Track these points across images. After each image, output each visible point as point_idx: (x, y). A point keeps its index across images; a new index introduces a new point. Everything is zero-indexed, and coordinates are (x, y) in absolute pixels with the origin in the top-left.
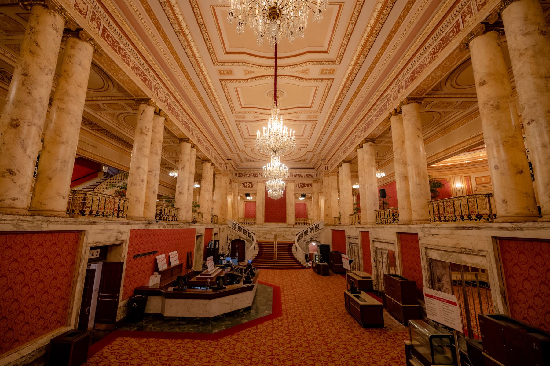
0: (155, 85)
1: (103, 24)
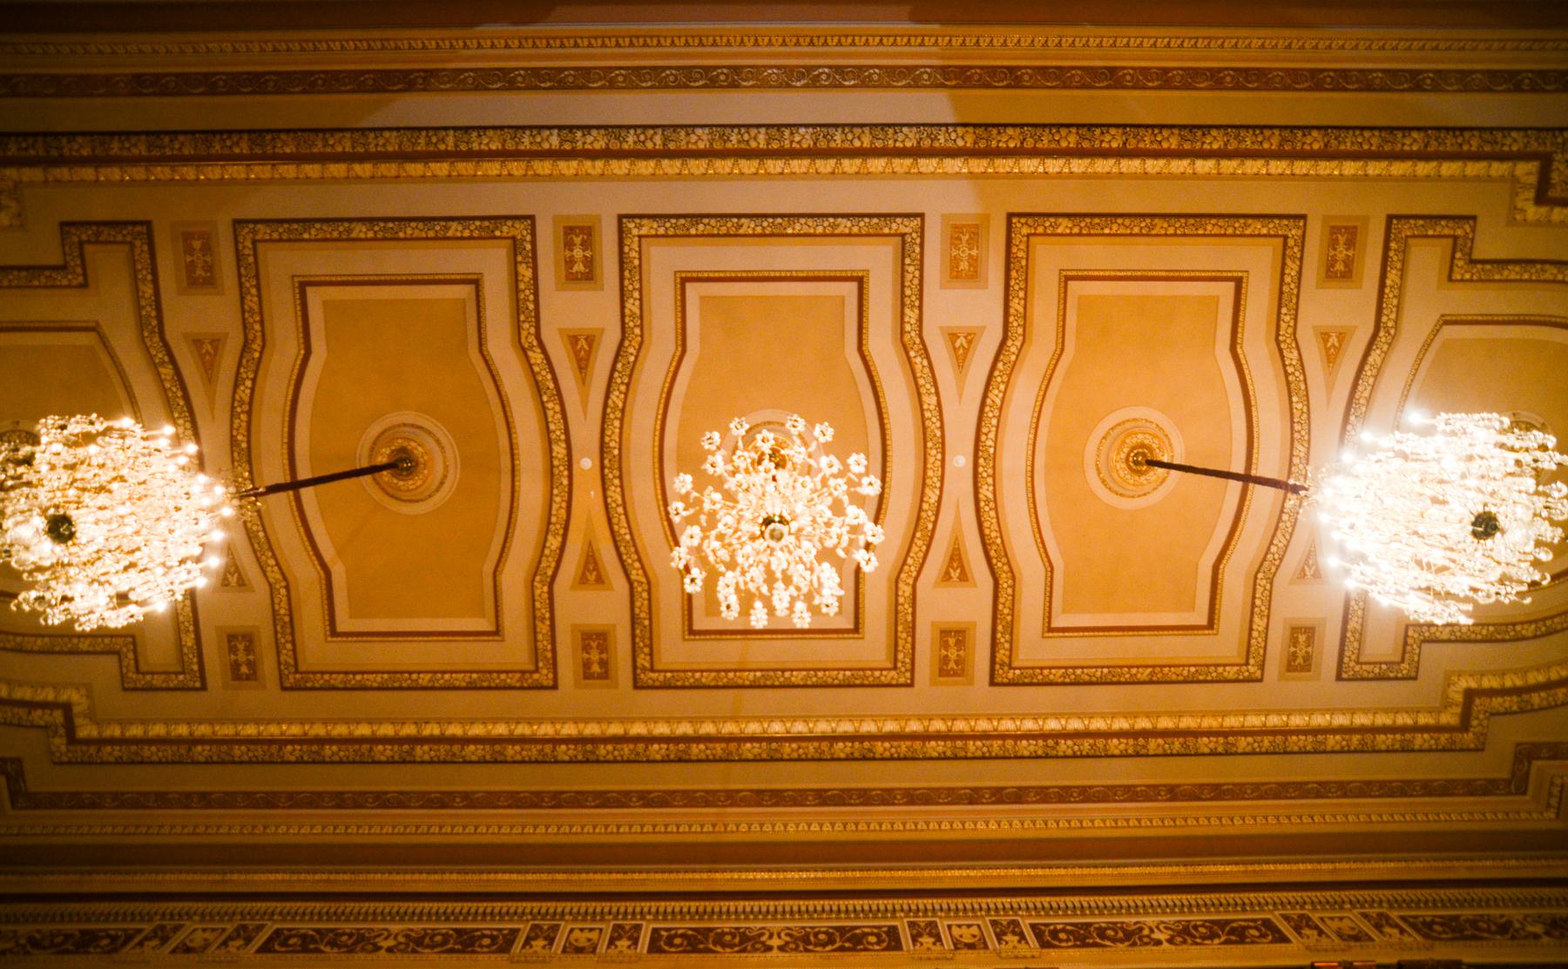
1: (1025, 924)
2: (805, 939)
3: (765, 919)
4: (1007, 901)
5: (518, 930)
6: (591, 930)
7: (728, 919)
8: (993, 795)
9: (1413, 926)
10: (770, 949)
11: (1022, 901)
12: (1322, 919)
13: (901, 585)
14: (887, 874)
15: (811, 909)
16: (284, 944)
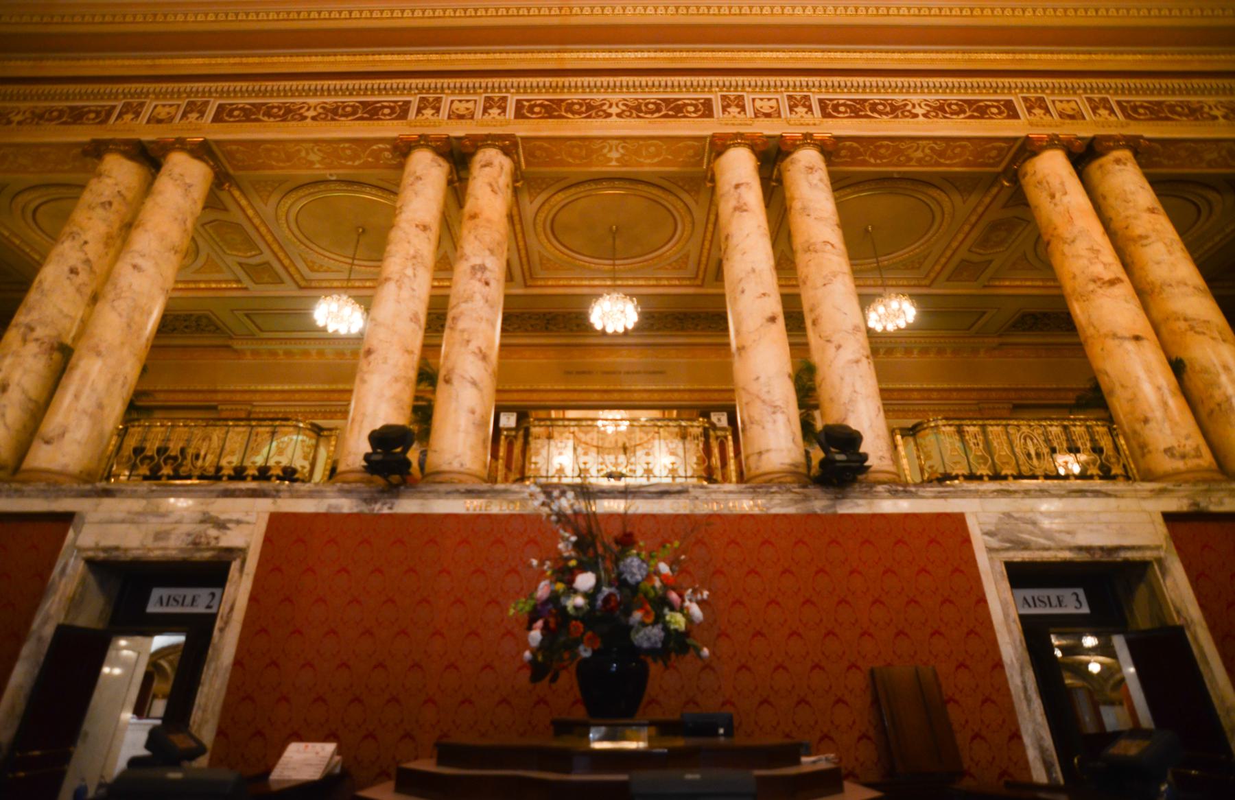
2: (638, 108)
3: (606, 92)
4: (804, 79)
5: (409, 102)
6: (468, 101)
7: (576, 93)
9: (1123, 109)
10: (609, 115)
11: (816, 79)
12: (1053, 102)
14: (710, 55)
15: (644, 84)
16: (230, 114)
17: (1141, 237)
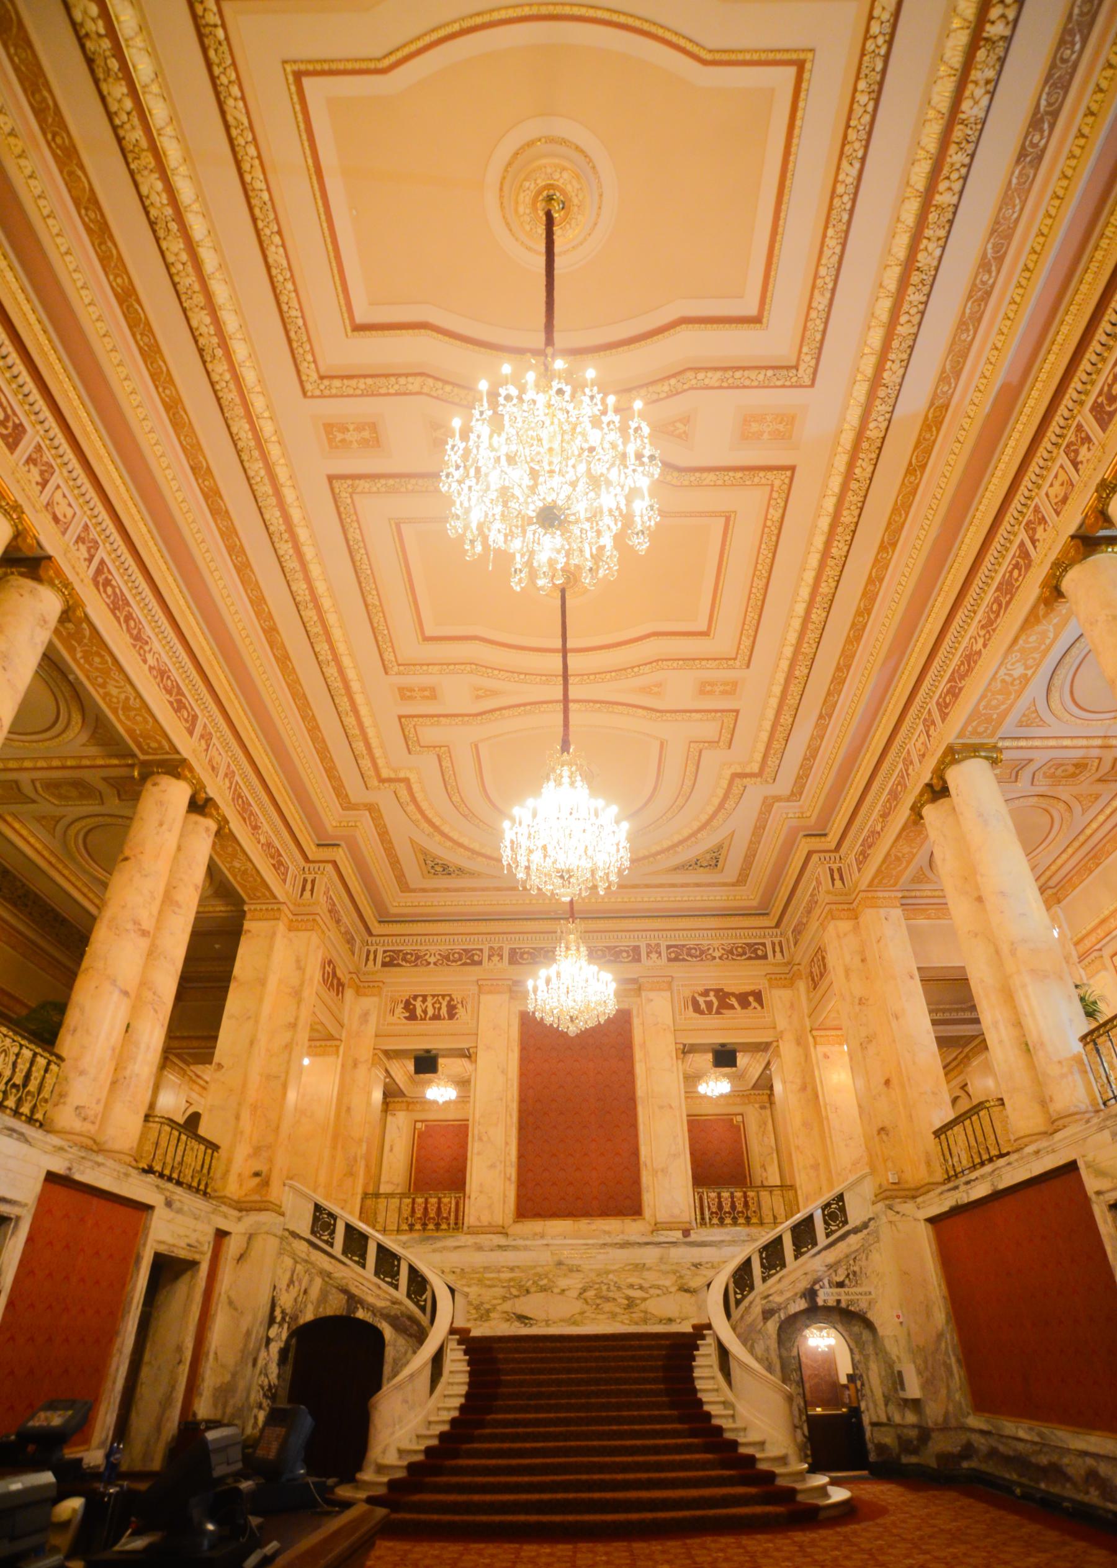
0: (205, 726)
1: (101, 553)
4: (112, 528)
8: (211, 489)
9: (235, 790)
13: (419, 379)
17: (177, 902)
